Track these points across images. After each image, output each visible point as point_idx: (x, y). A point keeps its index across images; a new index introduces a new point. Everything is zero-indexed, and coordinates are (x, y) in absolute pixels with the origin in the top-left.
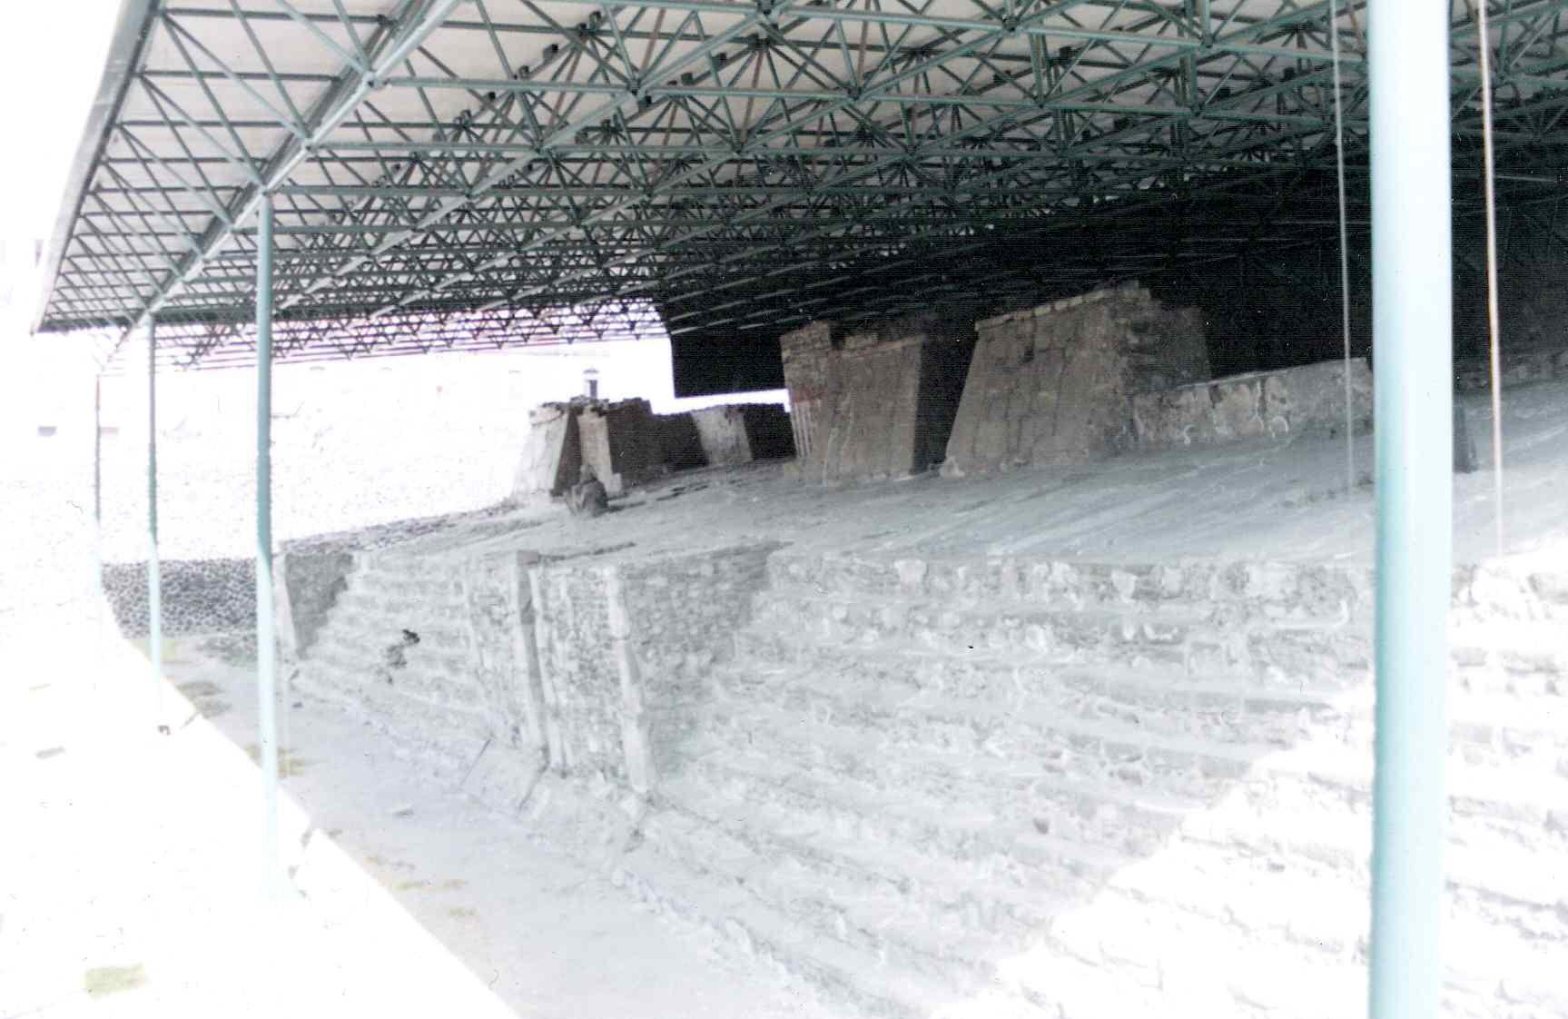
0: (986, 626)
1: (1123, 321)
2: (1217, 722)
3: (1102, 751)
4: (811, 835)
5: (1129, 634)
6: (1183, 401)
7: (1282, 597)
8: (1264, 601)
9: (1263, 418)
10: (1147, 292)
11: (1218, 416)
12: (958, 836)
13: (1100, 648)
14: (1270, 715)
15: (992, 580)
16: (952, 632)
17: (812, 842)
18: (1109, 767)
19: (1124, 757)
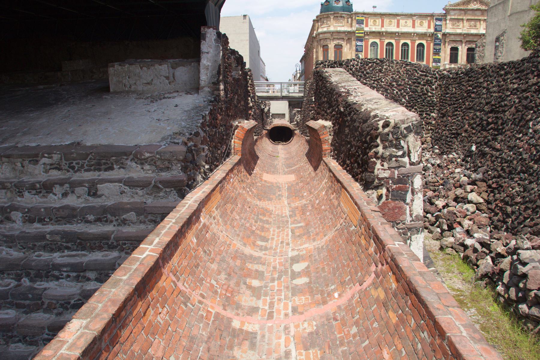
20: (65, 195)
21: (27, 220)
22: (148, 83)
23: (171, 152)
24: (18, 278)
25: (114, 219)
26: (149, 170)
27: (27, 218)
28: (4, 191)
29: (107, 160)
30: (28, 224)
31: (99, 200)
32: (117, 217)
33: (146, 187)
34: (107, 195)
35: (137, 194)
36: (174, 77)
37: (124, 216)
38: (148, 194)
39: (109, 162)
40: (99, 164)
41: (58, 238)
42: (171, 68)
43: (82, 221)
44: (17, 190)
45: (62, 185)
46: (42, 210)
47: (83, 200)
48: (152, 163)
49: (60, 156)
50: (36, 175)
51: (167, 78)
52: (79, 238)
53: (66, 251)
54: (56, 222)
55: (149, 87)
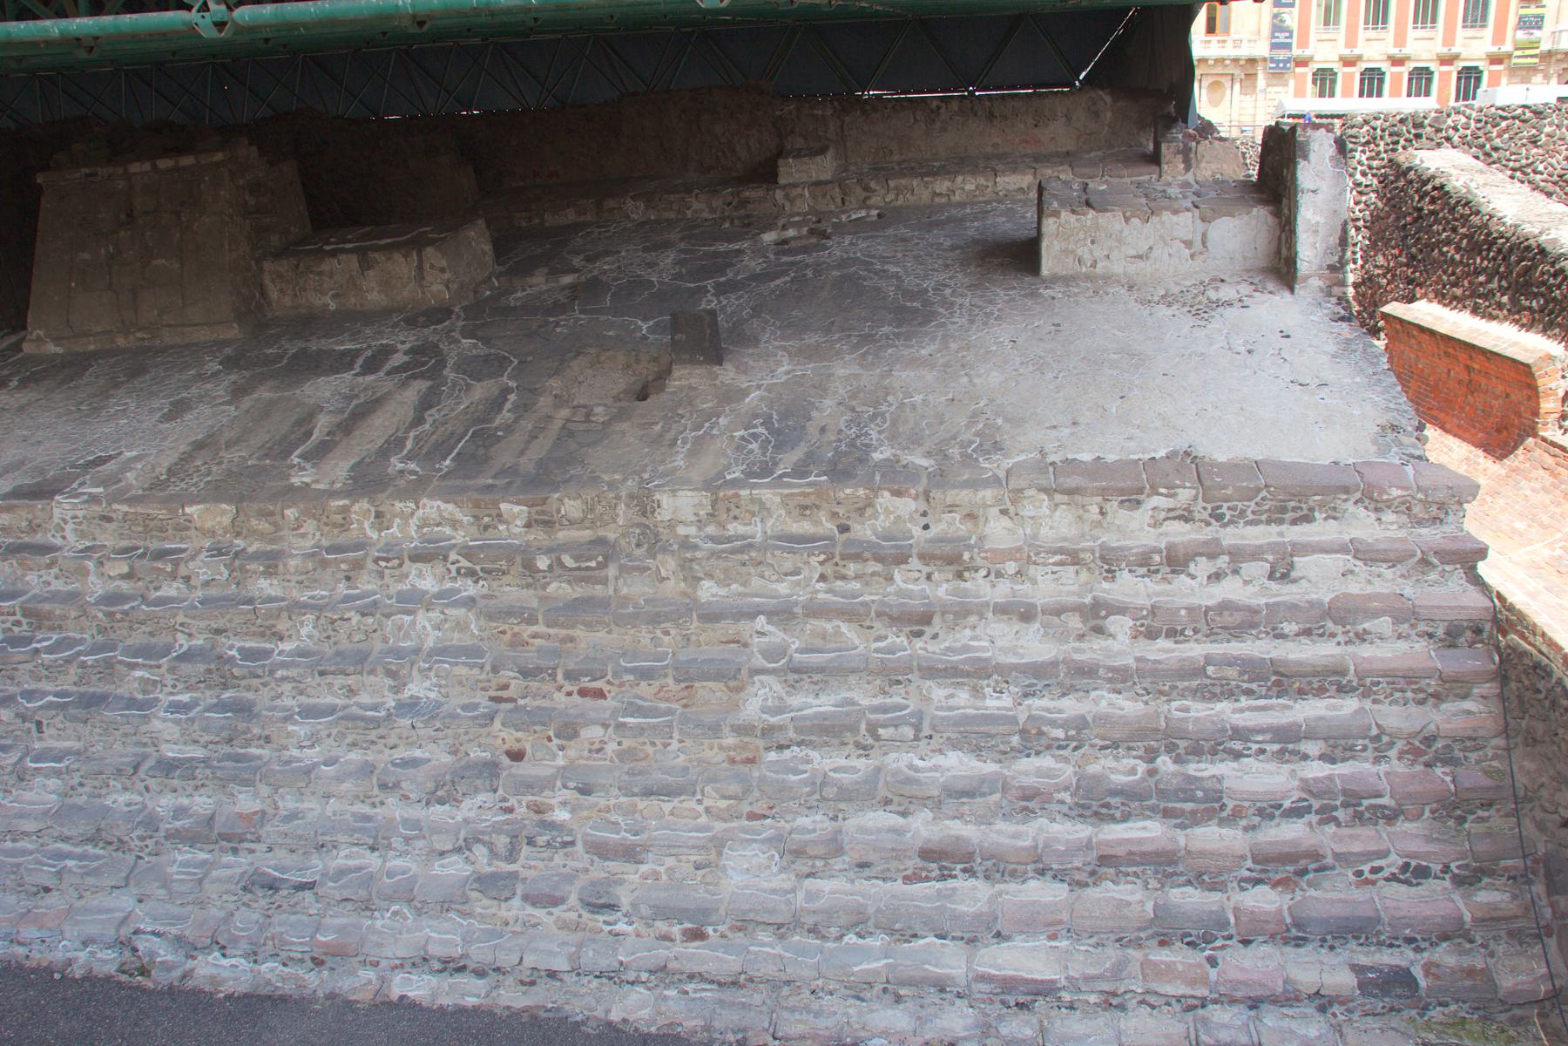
0: (353, 569)
1: (241, 182)
2: (667, 633)
3: (560, 677)
4: (212, 818)
5: (543, 563)
6: (325, 267)
7: (694, 518)
8: (672, 524)
9: (421, 286)
10: (254, 148)
11: (371, 281)
12: (431, 786)
13: (506, 579)
14: (723, 624)
15: (338, 518)
16: (300, 578)
17: (219, 827)
18: (568, 687)
19: (587, 679)
20: (1216, 577)
21: (1141, 633)
22: (1140, 257)
23: (1450, 488)
24: (1150, 756)
25: (1339, 629)
26: (1392, 523)
27: (1142, 629)
28: (1072, 569)
29: (1300, 501)
30: (1142, 642)
31: (1293, 588)
32: (1348, 627)
33: (1400, 562)
34: (1313, 579)
35: (1379, 576)
36: (1204, 243)
37: (1366, 625)
38: (1402, 576)
39: (1304, 506)
40: (1283, 510)
41: (1231, 672)
42: (1199, 221)
43: (1268, 633)
44: (1106, 567)
45: (1212, 556)
46: (1183, 612)
47: (1257, 589)
48: (1403, 508)
49: (1194, 492)
50: (1132, 531)
51: (1188, 244)
52: (1276, 673)
53: (1243, 698)
54: (1207, 636)
55: (1141, 264)
